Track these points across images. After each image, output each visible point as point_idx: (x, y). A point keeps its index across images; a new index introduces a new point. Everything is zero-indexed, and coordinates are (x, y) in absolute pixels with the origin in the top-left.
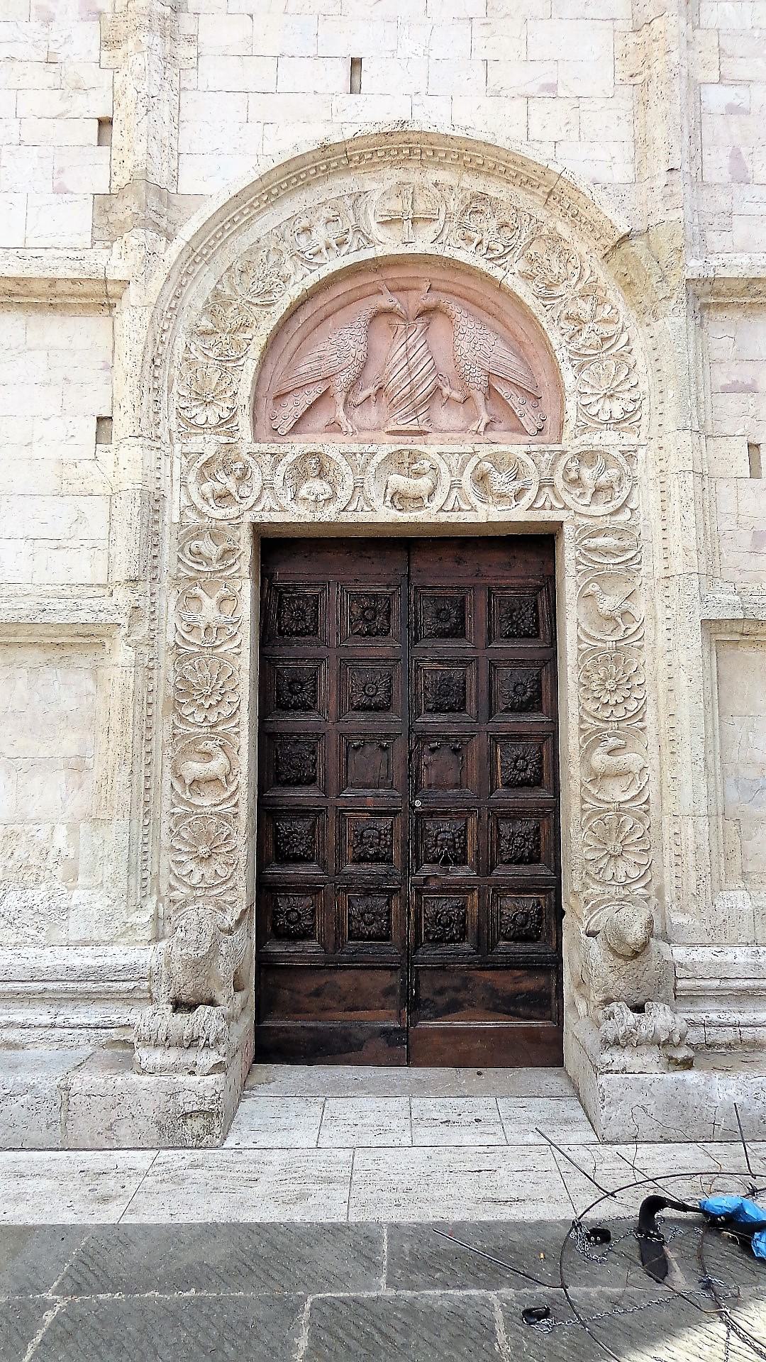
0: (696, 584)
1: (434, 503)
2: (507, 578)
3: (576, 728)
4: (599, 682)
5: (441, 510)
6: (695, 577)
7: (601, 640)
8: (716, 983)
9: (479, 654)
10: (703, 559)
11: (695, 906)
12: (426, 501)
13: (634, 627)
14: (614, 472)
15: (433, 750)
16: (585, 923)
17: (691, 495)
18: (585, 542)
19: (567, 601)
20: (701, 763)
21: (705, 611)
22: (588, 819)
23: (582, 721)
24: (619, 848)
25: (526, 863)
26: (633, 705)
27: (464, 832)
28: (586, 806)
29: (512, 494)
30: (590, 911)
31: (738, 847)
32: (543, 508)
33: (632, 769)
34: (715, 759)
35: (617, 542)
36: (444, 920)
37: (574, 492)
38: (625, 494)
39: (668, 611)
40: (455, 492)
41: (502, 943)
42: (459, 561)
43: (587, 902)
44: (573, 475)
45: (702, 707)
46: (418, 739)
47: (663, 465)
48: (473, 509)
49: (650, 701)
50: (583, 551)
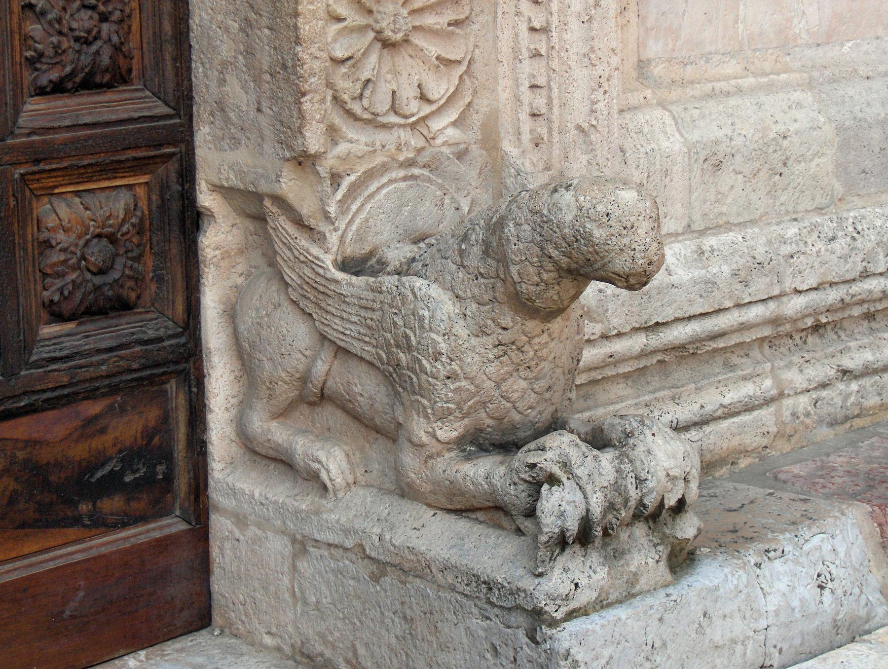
8: (639, 342)
11: (584, 158)
30: (343, 203)
41: (48, 330)
43: (336, 178)
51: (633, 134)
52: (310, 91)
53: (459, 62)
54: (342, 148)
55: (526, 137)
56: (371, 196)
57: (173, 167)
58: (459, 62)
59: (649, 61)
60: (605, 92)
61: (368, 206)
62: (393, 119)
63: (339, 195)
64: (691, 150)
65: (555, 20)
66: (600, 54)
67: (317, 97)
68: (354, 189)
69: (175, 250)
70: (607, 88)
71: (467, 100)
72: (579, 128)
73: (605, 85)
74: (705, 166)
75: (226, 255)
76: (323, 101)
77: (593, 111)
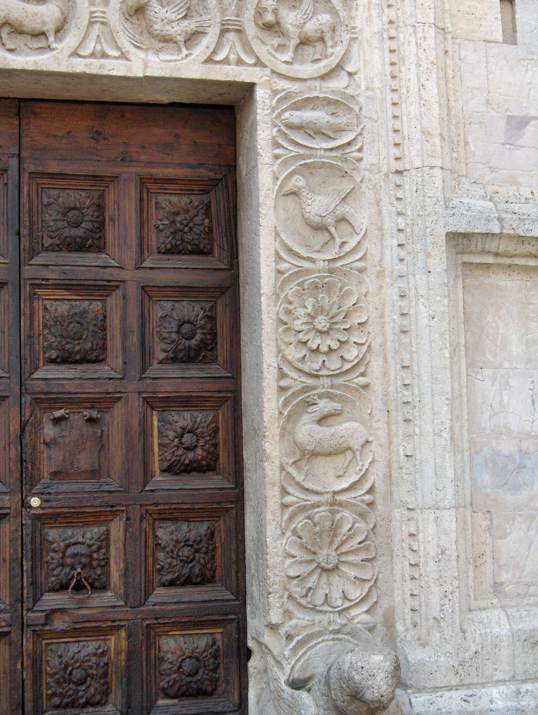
0: (439, 182)
1: (64, 43)
2: (167, 165)
3: (274, 387)
4: (305, 320)
5: (75, 54)
6: (437, 172)
7: (309, 259)
9: (127, 275)
10: (447, 149)
11: (438, 635)
12: (52, 39)
13: (353, 242)
14: (325, 18)
15: (57, 421)
16: (288, 669)
17: (432, 56)
18: (287, 115)
19: (261, 199)
20: (446, 435)
21: (451, 220)
22: (291, 518)
23: (282, 375)
24: (334, 559)
25: (196, 584)
26: (352, 353)
27: (105, 539)
28: (288, 499)
29: (181, 39)
30: (294, 650)
31: (489, 549)
32: (226, 61)
33: (351, 444)
34: (462, 427)
35: (328, 118)
36: (78, 674)
37: (269, 42)
38: (340, 50)
39: (400, 220)
40: (97, 29)
41: (162, 702)
42: (97, 136)
43: (289, 637)
44: (269, 18)
45: (447, 355)
46: (37, 401)
47: (392, 14)
48: (124, 56)
49: (375, 346)
50: (283, 128)
51: (476, 624)
52: (273, 592)
53: (369, 580)
54: (294, 622)
55: (409, 622)
56: (312, 647)
57: (234, 625)
58: (369, 580)
59: (502, 584)
60: (450, 600)
61: (309, 653)
62: (326, 608)
63: (291, 646)
64: (514, 635)
65: (422, 560)
66: (445, 579)
67: (278, 595)
68: (301, 644)
69: (234, 667)
70: (451, 598)
71: (375, 600)
72: (435, 618)
73: (450, 596)
74: (525, 643)
75: (259, 673)
76: (282, 597)
77: (441, 610)
